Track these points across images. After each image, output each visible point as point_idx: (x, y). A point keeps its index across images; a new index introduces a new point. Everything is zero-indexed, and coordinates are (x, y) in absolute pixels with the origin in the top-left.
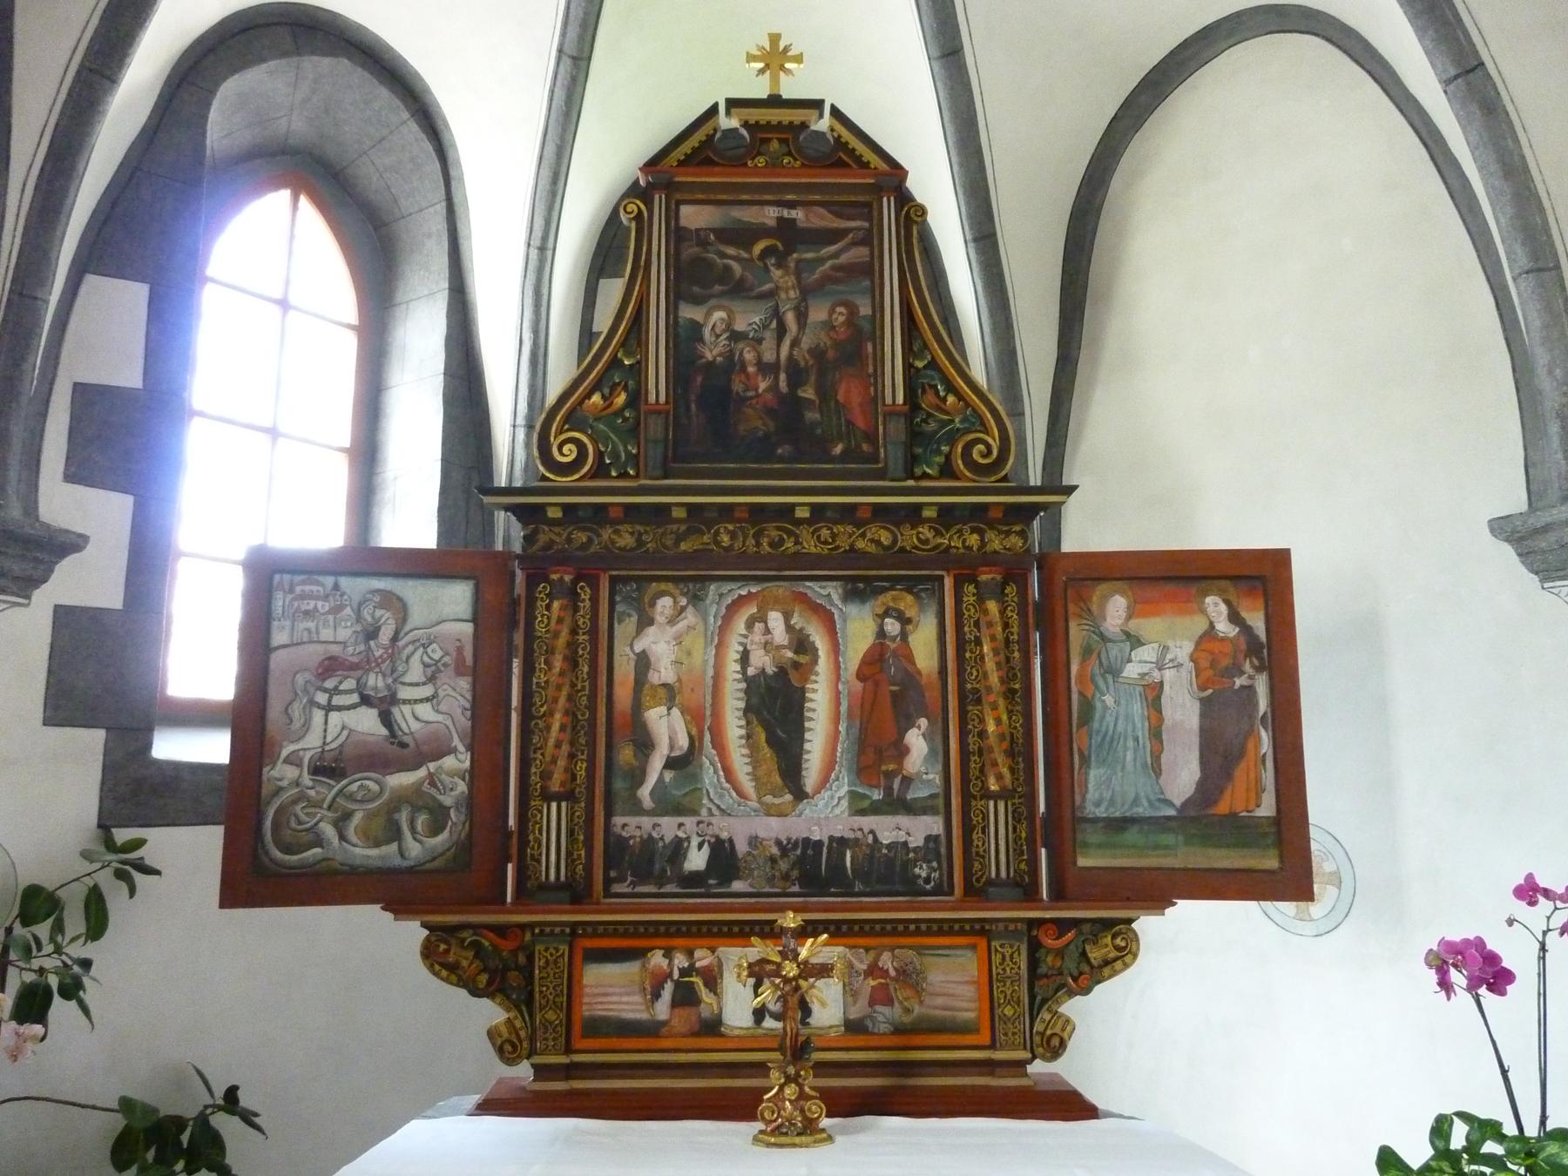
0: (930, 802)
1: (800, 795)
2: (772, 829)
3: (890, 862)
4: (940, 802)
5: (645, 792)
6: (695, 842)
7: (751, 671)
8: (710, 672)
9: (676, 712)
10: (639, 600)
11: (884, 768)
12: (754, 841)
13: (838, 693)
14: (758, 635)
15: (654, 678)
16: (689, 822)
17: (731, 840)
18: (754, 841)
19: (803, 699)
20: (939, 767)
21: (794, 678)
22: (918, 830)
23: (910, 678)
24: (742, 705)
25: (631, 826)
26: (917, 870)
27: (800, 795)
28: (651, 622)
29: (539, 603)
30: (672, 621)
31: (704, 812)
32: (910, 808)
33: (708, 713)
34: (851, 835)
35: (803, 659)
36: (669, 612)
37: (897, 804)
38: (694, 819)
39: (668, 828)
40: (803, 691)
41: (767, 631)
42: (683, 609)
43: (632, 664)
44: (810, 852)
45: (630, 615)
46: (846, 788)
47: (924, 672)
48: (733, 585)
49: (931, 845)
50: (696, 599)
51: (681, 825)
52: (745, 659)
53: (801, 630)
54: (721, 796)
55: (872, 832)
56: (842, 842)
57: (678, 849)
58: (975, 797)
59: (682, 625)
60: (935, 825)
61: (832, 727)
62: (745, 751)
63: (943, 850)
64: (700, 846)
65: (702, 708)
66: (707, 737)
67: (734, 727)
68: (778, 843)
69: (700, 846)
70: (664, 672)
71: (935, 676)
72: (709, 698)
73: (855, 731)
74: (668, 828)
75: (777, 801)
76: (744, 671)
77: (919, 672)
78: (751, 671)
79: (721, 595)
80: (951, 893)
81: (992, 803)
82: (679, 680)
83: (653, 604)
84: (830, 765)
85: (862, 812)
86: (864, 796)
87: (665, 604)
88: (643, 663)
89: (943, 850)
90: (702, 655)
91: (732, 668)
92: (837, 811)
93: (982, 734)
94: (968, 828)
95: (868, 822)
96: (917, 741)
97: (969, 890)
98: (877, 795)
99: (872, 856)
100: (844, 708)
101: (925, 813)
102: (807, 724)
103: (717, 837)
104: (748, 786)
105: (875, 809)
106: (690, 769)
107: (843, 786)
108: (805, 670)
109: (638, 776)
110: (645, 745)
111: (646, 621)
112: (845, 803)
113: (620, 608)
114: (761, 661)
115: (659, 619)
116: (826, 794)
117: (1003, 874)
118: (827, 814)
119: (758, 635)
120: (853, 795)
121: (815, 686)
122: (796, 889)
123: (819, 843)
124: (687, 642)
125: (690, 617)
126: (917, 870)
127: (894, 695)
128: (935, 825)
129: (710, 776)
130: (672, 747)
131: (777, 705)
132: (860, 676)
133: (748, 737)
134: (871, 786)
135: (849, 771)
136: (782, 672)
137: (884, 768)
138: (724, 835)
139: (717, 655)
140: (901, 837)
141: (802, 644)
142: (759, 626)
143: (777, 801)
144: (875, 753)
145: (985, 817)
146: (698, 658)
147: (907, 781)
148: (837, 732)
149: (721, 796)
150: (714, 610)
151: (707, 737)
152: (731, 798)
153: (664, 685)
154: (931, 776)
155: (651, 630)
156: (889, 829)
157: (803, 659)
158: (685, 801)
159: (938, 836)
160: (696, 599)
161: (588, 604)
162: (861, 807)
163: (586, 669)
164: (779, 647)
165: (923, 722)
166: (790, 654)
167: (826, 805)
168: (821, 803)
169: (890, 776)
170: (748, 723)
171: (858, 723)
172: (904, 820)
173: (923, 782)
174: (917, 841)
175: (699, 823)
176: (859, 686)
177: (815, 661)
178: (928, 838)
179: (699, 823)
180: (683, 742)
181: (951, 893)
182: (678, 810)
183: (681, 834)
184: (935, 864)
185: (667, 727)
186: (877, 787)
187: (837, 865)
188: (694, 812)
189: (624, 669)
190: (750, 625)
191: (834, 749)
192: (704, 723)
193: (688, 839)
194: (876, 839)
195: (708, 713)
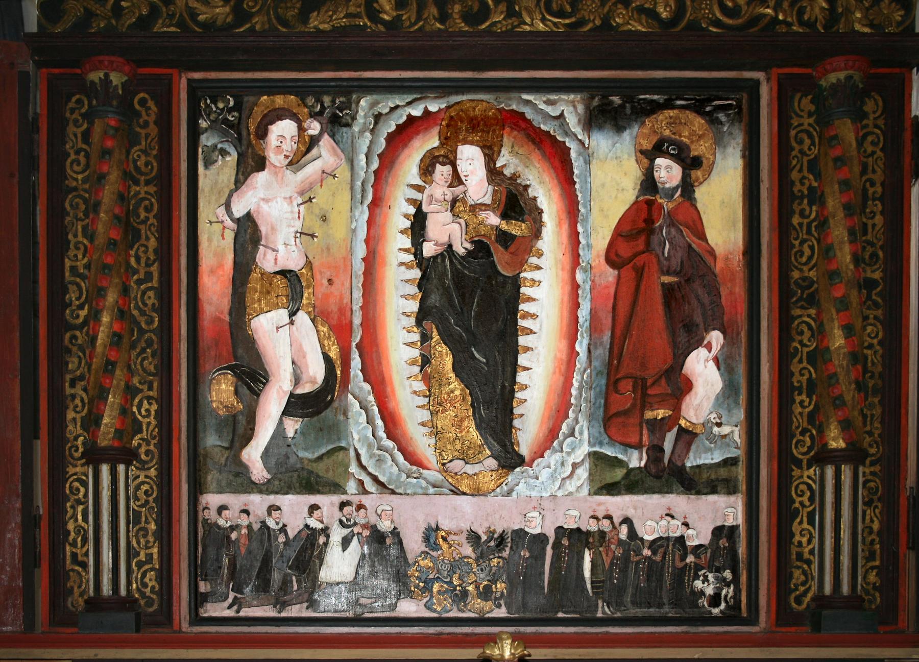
0: (723, 473)
1: (510, 460)
2: (462, 514)
3: (654, 570)
4: (741, 472)
5: (253, 455)
6: (337, 534)
7: (429, 250)
8: (361, 251)
9: (302, 317)
10: (236, 126)
11: (649, 415)
12: (431, 535)
13: (575, 287)
14: (440, 188)
15: (267, 261)
16: (328, 502)
17: (395, 533)
18: (431, 535)
19: (515, 298)
20: (740, 414)
21: (500, 258)
22: (702, 517)
23: (697, 263)
24: (413, 306)
25: (226, 507)
26: (698, 584)
27: (510, 460)
28: (261, 164)
29: (71, 129)
30: (295, 163)
31: (351, 487)
32: (691, 483)
33: (357, 320)
34: (593, 526)
35: (517, 229)
36: (289, 146)
37: (669, 476)
38: (336, 499)
39: (293, 511)
40: (516, 283)
41: (457, 179)
42: (314, 141)
43: (230, 236)
44: (525, 553)
45: (224, 153)
46: (585, 449)
47: (719, 251)
48: (398, 100)
49: (723, 543)
50: (336, 123)
51: (314, 508)
52: (418, 226)
53: (514, 177)
54: (380, 461)
55: (627, 521)
56: (574, 539)
57: (309, 550)
58: (798, 463)
59: (311, 170)
60: (729, 509)
61: (564, 345)
62: (420, 386)
63: (742, 550)
64: (346, 543)
65: (345, 311)
66: (356, 362)
67: (400, 344)
68: (473, 537)
69: (346, 543)
70: (281, 252)
71: (737, 258)
72: (358, 294)
73: (602, 353)
74: (293, 511)
75: (470, 469)
76: (417, 250)
77: (712, 252)
78: (429, 250)
79: (378, 117)
80: (752, 620)
81: (830, 471)
82: (309, 264)
83: (262, 133)
84: (560, 409)
85: (611, 489)
86: (616, 462)
87: (283, 132)
88: (248, 233)
89: (742, 550)
90: (348, 224)
91: (397, 243)
92: (571, 486)
93: (819, 356)
94: (785, 514)
95: (620, 505)
96: (703, 369)
97: (784, 615)
98: (636, 460)
99: (626, 558)
100: (584, 313)
101: (714, 491)
102: (522, 340)
103: (374, 529)
104: (423, 443)
105: (633, 484)
106: (328, 413)
107: (580, 444)
108: (522, 248)
109: (241, 428)
110: (252, 376)
111: (252, 162)
112: (583, 473)
113: (207, 140)
114: (444, 231)
115: (275, 158)
116: (552, 458)
117: (845, 589)
118: (554, 492)
119: (440, 188)
120: (597, 458)
121: (536, 275)
122: (502, 613)
123: (541, 539)
124: (322, 198)
125: (326, 155)
126: (698, 584)
127: (669, 292)
128: (729, 509)
129: (360, 428)
130: (297, 381)
131: (472, 303)
132: (612, 257)
133: (425, 360)
134: (627, 445)
135: (591, 418)
136: (480, 249)
137: (649, 415)
138: (385, 526)
139: (370, 222)
140: (675, 529)
141: (514, 202)
142: (442, 172)
143: (470, 469)
144: (632, 387)
145: (818, 497)
146: (338, 229)
147: (687, 436)
148: (573, 354)
149: (380, 461)
150: (367, 142)
151: (356, 362)
152: (391, 469)
153: (284, 273)
154: (726, 430)
155: (260, 178)
156: (653, 516)
157: (517, 229)
158: (320, 468)
159: (733, 529)
160: (336, 123)
161: (153, 130)
162: (610, 479)
163: (153, 243)
164: (475, 209)
165: (716, 338)
166: (493, 219)
167: (553, 477)
168: (545, 474)
169: (658, 427)
170: (425, 338)
171: (607, 337)
172: (679, 502)
173: (712, 438)
174: (699, 536)
175: (343, 505)
176: (611, 274)
177: (537, 234)
178: (718, 532)
179: (343, 505)
180: (316, 371)
181: (752, 620)
182: (309, 483)
183: (314, 524)
184: (728, 574)
185: (290, 347)
186: (638, 446)
187: (566, 579)
188: (336, 488)
189: (216, 247)
190: (427, 170)
191: (567, 384)
192: (353, 338)
193: (326, 531)
194: (632, 533)
195: (357, 320)
